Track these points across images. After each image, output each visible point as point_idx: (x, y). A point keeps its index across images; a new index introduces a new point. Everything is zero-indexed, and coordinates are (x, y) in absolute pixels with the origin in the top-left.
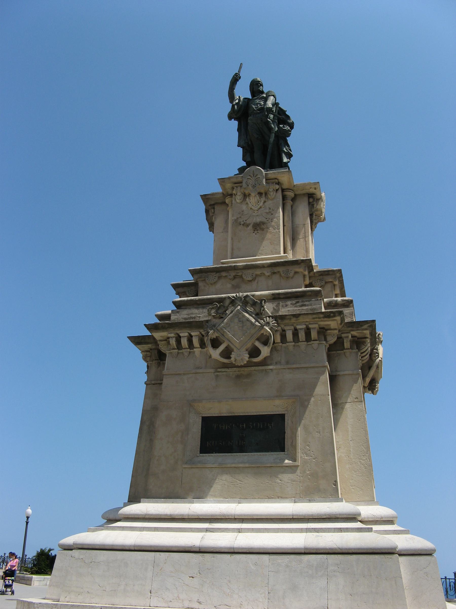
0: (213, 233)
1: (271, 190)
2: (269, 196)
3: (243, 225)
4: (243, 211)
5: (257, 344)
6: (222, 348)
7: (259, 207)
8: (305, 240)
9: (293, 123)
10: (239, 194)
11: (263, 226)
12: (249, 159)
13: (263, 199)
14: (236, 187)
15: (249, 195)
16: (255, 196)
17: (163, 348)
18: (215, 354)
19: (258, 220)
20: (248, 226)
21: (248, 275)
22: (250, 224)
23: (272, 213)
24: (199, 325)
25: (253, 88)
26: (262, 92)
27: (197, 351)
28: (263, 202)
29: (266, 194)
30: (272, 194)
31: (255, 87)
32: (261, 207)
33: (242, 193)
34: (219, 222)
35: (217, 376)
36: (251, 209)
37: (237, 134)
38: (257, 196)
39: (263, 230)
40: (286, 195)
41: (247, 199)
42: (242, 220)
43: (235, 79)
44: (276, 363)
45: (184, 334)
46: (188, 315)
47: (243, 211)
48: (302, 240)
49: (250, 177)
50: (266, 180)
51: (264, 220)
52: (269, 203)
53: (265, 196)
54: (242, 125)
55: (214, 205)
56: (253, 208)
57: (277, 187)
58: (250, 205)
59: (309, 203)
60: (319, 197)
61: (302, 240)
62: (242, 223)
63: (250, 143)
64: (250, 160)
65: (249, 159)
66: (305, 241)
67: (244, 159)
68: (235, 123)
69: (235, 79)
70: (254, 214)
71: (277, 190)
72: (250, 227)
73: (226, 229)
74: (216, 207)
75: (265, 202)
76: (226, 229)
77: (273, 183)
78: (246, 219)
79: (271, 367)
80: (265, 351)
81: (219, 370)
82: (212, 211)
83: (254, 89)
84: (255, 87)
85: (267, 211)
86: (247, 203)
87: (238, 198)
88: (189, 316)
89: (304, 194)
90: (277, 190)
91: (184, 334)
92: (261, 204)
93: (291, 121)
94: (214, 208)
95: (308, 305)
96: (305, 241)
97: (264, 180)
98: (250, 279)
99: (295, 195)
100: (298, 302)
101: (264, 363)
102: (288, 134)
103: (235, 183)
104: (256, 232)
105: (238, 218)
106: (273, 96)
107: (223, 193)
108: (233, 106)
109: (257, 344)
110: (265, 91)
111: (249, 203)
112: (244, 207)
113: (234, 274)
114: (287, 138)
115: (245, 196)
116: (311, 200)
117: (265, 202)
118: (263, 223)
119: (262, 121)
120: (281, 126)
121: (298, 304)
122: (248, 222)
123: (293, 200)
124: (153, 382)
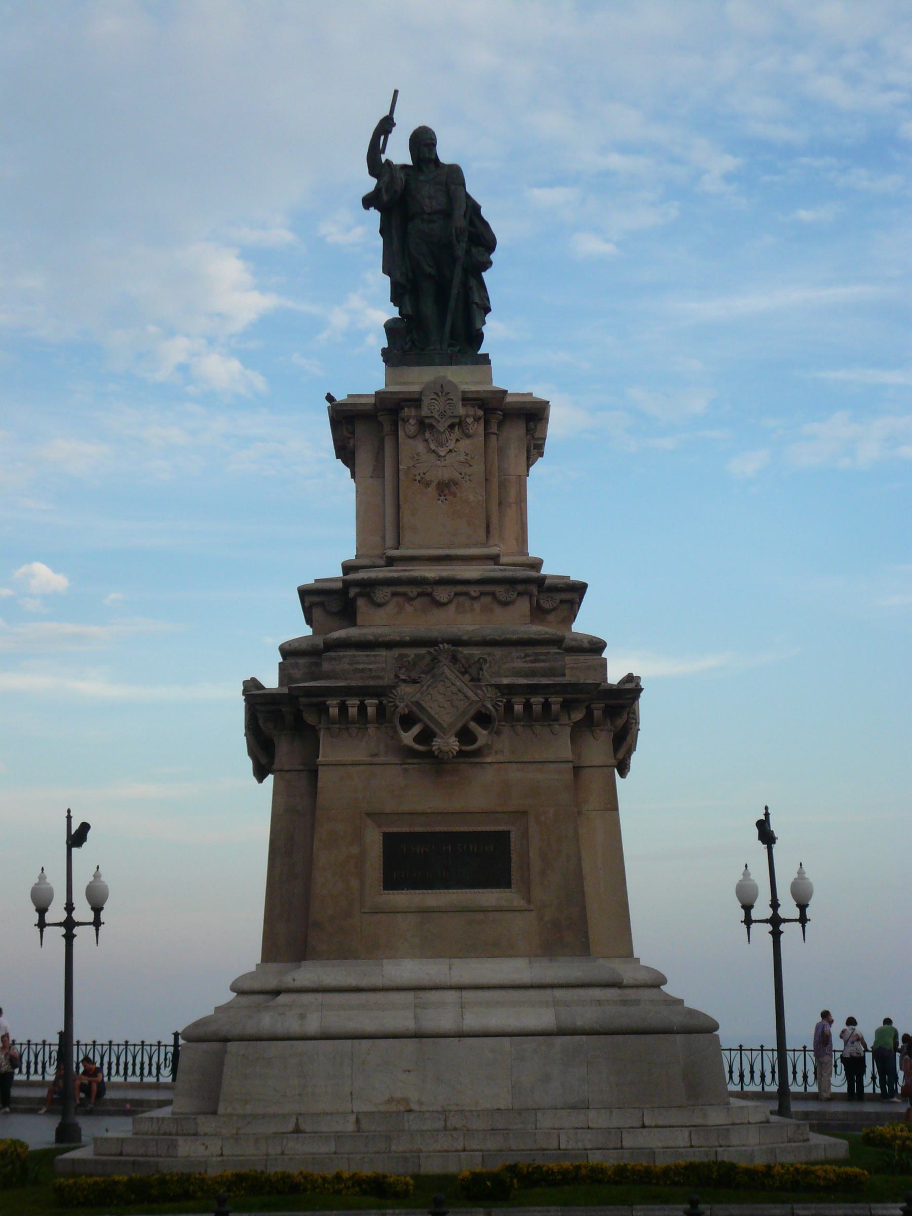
0: (346, 463)
5: (473, 725)
6: (416, 729)
10: (412, 421)
11: (453, 488)
12: (409, 310)
17: (310, 718)
18: (408, 738)
19: (446, 477)
20: (428, 484)
21: (442, 594)
22: (431, 481)
24: (379, 692)
27: (372, 729)
28: (454, 441)
32: (450, 451)
34: (364, 457)
35: (406, 770)
37: (379, 242)
39: (455, 495)
41: (427, 435)
44: (496, 752)
45: (353, 703)
46: (351, 664)
48: (514, 506)
51: (457, 476)
52: (465, 444)
59: (528, 430)
61: (514, 506)
62: (418, 478)
71: (479, 419)
75: (457, 440)
79: (489, 760)
80: (483, 735)
85: (462, 458)
88: (353, 667)
95: (543, 661)
98: (446, 600)
100: (526, 656)
101: (478, 753)
104: (442, 498)
105: (409, 467)
107: (375, 404)
109: (473, 725)
113: (419, 590)
116: (532, 425)
117: (457, 440)
118: (456, 484)
120: (474, 250)
121: (528, 659)
122: (428, 477)
124: (286, 768)
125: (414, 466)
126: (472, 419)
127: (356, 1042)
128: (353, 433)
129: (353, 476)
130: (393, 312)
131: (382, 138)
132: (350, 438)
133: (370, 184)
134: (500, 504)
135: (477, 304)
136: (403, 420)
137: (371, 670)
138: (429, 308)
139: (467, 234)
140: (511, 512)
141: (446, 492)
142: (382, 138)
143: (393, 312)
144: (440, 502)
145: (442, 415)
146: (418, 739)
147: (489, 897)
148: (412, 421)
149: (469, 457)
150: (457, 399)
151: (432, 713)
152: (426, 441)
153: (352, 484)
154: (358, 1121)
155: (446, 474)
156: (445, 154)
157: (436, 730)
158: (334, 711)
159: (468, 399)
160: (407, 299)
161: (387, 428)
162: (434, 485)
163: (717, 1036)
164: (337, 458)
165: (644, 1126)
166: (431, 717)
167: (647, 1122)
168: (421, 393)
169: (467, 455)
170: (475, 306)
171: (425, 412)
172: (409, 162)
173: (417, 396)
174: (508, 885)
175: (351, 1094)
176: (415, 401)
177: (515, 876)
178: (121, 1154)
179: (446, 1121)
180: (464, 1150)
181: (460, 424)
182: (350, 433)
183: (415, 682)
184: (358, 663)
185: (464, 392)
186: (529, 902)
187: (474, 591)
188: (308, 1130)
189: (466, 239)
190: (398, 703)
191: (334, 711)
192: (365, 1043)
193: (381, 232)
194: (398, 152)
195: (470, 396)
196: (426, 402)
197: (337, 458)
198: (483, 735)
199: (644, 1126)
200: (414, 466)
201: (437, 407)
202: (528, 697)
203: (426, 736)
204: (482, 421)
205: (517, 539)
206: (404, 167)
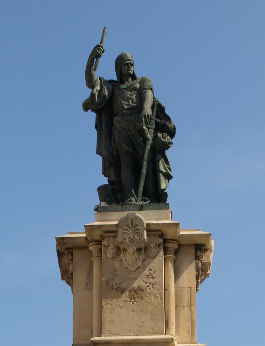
1: (153, 245)
2: (150, 254)
3: (116, 289)
4: (115, 271)
7: (137, 267)
8: (191, 309)
9: (174, 129)
10: (111, 247)
12: (113, 178)
13: (142, 256)
14: (108, 237)
15: (125, 250)
16: (134, 253)
23: (154, 275)
25: (121, 70)
26: (134, 77)
28: (141, 260)
29: (146, 248)
30: (153, 250)
31: (122, 64)
32: (139, 267)
33: (115, 246)
34: (79, 277)
36: (126, 268)
37: (94, 133)
38: (136, 253)
39: (142, 298)
40: (168, 248)
41: (122, 255)
42: (114, 283)
43: (96, 54)
47: (115, 271)
49: (127, 228)
50: (147, 231)
53: (145, 253)
54: (104, 123)
55: (71, 248)
56: (129, 267)
57: (161, 241)
58: (125, 264)
60: (206, 248)
61: (186, 309)
62: (115, 287)
63: (115, 154)
64: (115, 180)
65: (113, 178)
66: (191, 310)
67: (105, 173)
68: (92, 116)
69: (96, 54)
70: (130, 276)
73: (89, 286)
74: (74, 252)
75: (144, 260)
76: (89, 286)
77: (155, 236)
78: (120, 282)
82: (70, 257)
83: (123, 72)
84: (122, 64)
86: (121, 260)
87: (109, 252)
89: (190, 245)
90: (160, 245)
92: (140, 264)
93: (172, 126)
94: (72, 254)
96: (191, 310)
97: (145, 232)
99: (180, 245)
102: (167, 146)
103: (107, 232)
104: (133, 300)
105: (109, 279)
106: (151, 89)
107: (86, 238)
108: (93, 95)
110: (139, 76)
111: (124, 260)
112: (117, 265)
114: (166, 151)
115: (119, 250)
116: (199, 253)
118: (142, 291)
119: (134, 127)
120: (159, 135)
122: (122, 286)
123: (176, 252)
125: (112, 279)
126: (154, 245)
128: (72, 260)
129: (72, 293)
130: (105, 181)
131: (95, 59)
132: (69, 264)
133: (86, 93)
134: (176, 307)
135: (162, 172)
136: (105, 246)
139: (154, 123)
140: (185, 313)
142: (95, 59)
143: (105, 181)
145: (131, 241)
148: (111, 247)
149: (152, 272)
153: (70, 296)
156: (138, 70)
159: (150, 230)
160: (112, 171)
161: (95, 253)
164: (63, 279)
168: (117, 226)
169: (151, 270)
170: (161, 174)
171: (120, 238)
172: (116, 79)
173: (114, 229)
176: (111, 232)
181: (146, 248)
182: (70, 260)
185: (148, 225)
189: (154, 127)
193: (96, 127)
194: (106, 71)
195: (152, 228)
196: (120, 231)
197: (63, 279)
200: (112, 279)
204: (162, 247)
205: (189, 332)
206: (111, 81)
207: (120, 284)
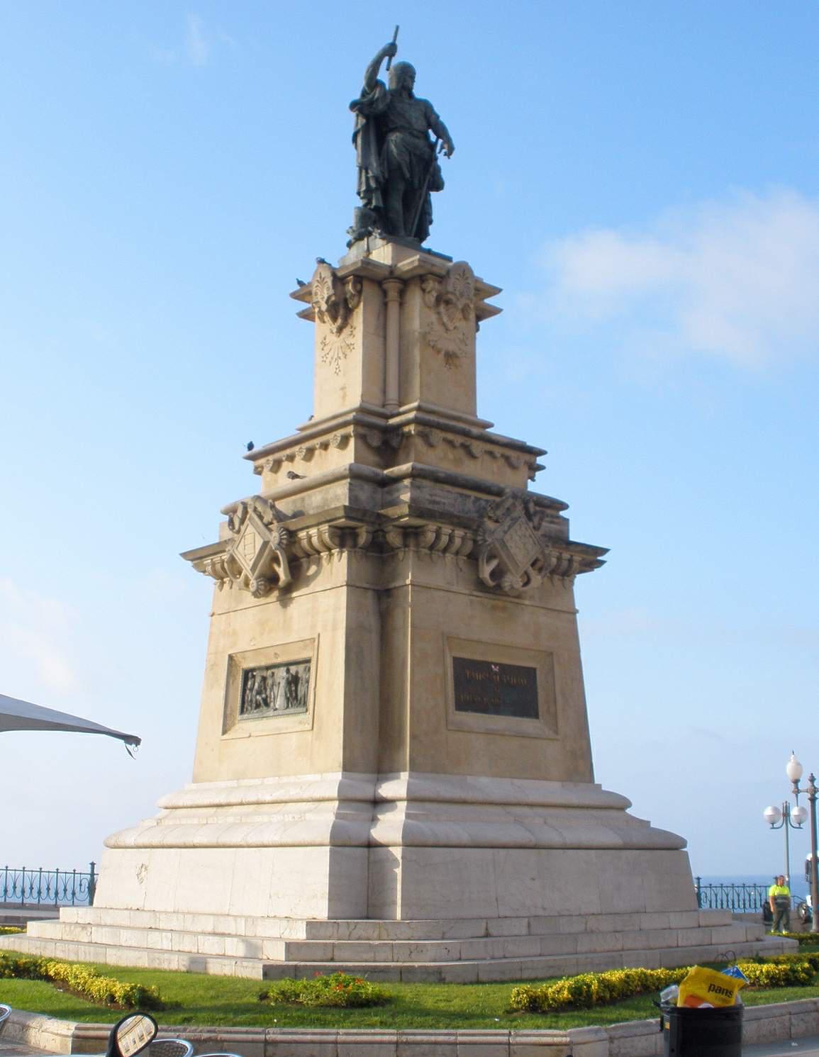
6: (494, 563)
20: (439, 352)
35: (472, 602)
46: (431, 495)
47: (432, 323)
62: (432, 344)
72: (441, 356)
80: (537, 580)
81: (475, 593)
91: (447, 530)
127: (496, 850)
137: (444, 504)
138: (397, 204)
141: (450, 362)
144: (446, 369)
146: (493, 574)
147: (527, 724)
150: (472, 286)
151: (512, 551)
152: (439, 313)
154: (529, 925)
155: (451, 347)
157: (511, 567)
158: (431, 537)
161: (393, 295)
162: (443, 353)
163: (686, 852)
165: (699, 926)
166: (511, 557)
167: (701, 924)
169: (464, 334)
174: (536, 716)
175: (497, 899)
177: (542, 708)
178: (332, 960)
179: (586, 924)
180: (623, 950)
183: (497, 521)
184: (436, 495)
186: (556, 732)
187: (498, 451)
188: (495, 934)
190: (487, 539)
191: (431, 537)
192: (502, 852)
196: (452, 279)
198: (537, 580)
199: (699, 926)
201: (458, 289)
202: (572, 554)
203: (497, 574)
207: (436, 341)
